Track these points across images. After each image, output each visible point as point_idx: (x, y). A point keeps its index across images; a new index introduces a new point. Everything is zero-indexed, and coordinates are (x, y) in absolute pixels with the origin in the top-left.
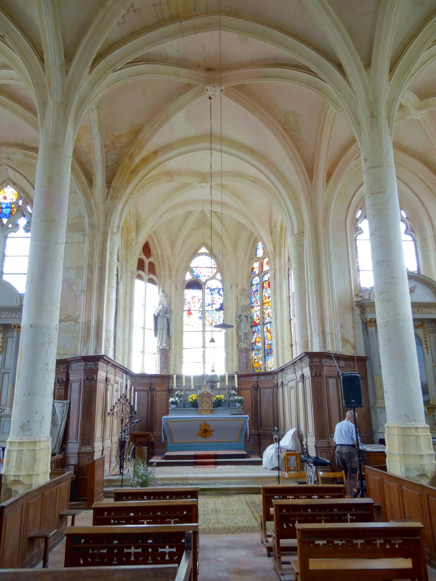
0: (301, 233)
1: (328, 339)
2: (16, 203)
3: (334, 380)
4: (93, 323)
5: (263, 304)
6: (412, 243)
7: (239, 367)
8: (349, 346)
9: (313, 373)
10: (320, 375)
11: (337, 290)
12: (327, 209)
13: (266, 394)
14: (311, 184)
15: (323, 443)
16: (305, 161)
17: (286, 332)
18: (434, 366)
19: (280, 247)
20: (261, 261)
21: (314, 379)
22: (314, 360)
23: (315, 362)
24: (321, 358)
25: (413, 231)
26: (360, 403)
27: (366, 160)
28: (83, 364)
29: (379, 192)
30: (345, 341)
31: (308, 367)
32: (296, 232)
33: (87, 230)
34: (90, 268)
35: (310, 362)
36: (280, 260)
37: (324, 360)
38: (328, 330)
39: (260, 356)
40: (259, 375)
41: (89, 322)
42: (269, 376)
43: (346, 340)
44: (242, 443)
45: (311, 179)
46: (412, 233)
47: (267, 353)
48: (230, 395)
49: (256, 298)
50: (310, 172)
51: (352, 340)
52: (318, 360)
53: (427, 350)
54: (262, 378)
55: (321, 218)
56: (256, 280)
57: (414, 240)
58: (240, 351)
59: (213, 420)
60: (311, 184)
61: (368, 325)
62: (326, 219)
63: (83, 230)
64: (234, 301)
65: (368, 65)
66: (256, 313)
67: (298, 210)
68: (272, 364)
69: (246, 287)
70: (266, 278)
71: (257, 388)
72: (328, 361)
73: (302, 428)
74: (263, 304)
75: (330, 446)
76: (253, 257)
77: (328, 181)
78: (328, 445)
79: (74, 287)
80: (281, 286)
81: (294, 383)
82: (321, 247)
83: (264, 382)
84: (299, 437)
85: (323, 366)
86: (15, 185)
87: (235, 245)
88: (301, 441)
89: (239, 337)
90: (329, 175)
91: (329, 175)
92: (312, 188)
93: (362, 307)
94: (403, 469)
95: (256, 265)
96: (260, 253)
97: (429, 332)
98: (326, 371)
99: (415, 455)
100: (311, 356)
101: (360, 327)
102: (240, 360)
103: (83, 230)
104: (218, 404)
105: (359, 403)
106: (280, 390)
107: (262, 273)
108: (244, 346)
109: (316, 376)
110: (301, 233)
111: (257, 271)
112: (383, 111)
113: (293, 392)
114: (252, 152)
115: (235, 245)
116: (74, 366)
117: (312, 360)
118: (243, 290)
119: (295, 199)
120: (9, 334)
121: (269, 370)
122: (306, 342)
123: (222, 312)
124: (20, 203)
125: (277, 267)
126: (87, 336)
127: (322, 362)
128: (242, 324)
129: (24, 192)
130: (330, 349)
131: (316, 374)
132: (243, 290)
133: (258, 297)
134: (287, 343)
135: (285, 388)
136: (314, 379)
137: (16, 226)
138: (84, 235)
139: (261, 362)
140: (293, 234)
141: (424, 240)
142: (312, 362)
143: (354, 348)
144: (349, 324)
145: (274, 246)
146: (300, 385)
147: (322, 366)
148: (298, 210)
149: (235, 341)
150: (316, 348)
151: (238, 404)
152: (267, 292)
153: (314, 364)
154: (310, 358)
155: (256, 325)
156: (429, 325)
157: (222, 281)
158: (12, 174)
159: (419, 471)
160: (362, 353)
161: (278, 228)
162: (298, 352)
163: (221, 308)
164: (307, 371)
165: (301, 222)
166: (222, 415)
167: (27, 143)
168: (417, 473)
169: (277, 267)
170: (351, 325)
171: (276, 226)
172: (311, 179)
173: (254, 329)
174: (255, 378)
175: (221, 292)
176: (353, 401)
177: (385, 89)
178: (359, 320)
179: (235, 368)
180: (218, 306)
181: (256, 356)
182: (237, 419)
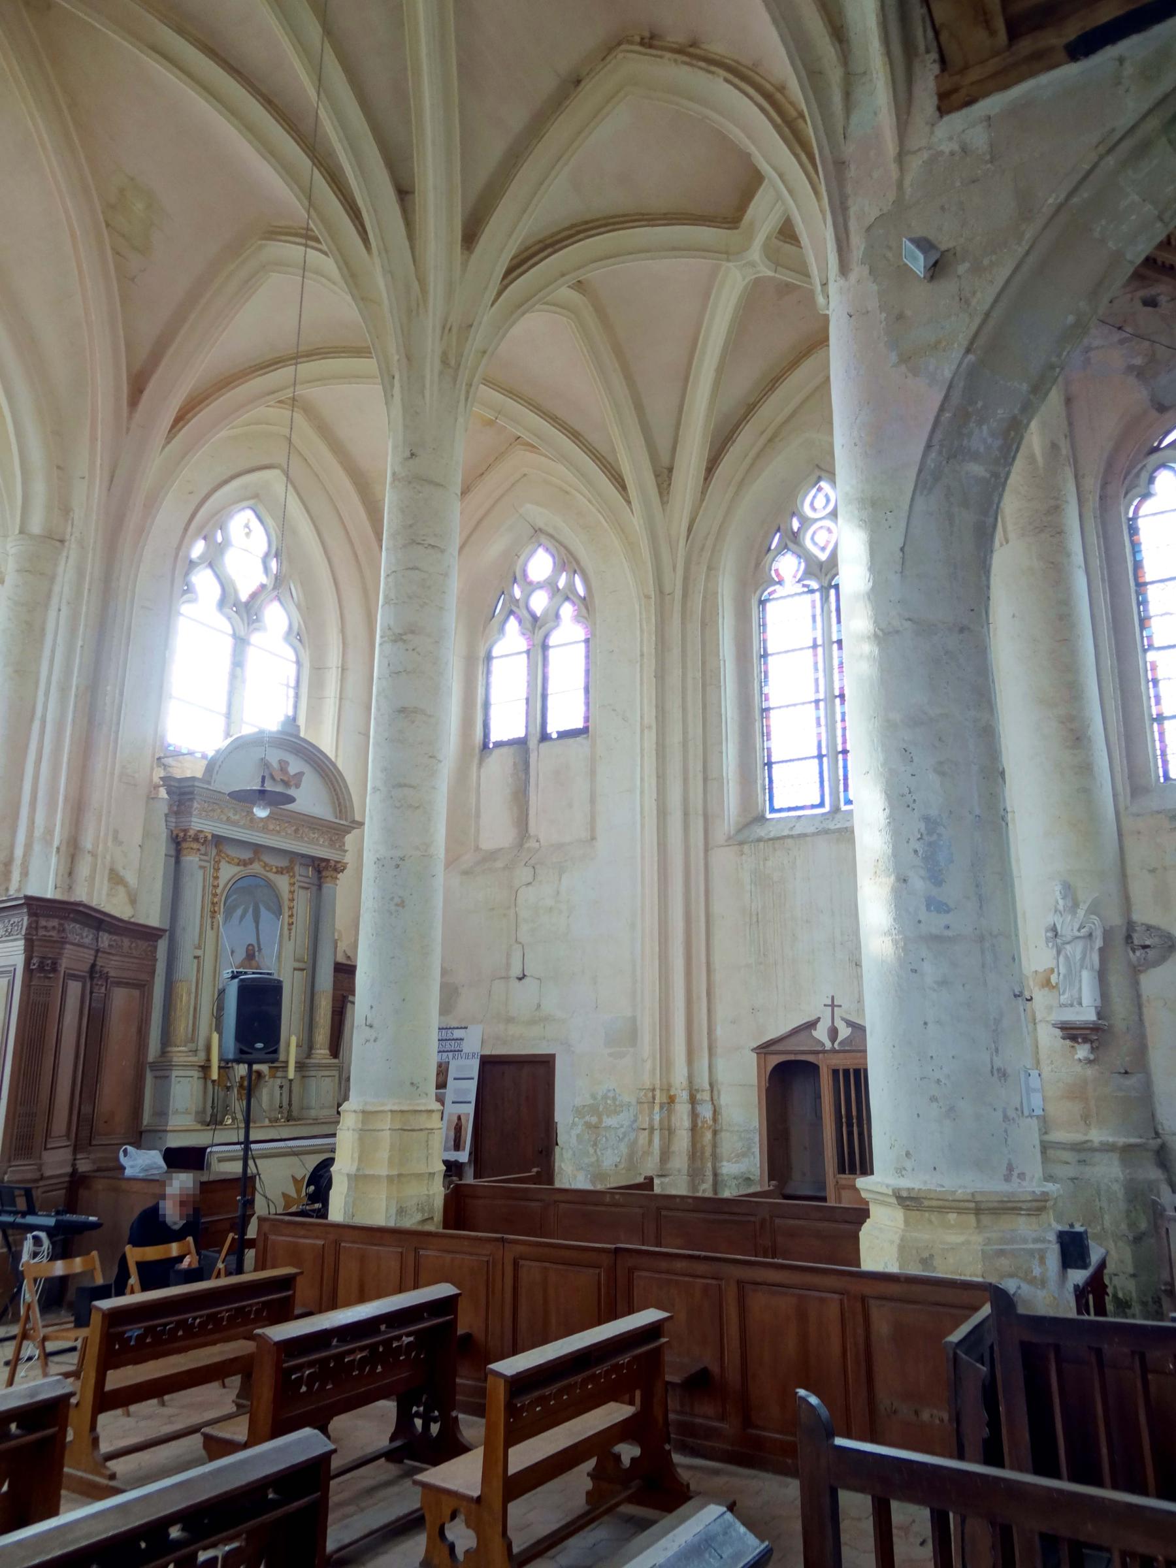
0: (54, 540)
1: (84, 869)
3: (79, 984)
6: (293, 668)
9: (35, 960)
10: (54, 969)
14: (130, 418)
18: (295, 969)
21: (31, 980)
22: (43, 922)
23: (45, 928)
24: (65, 918)
25: (300, 640)
26: (276, 1051)
27: (412, 455)
29: (433, 547)
31: (22, 942)
35: (29, 927)
37: (70, 926)
43: (117, 875)
45: (134, 402)
46: (297, 643)
51: (131, 878)
52: (55, 923)
53: (290, 930)
57: (298, 663)
60: (130, 418)
67: (58, 467)
72: (79, 931)
75: (42, 1178)
78: (36, 1175)
85: (65, 943)
90: (181, 419)
91: (181, 419)
92: (128, 429)
94: (393, 1211)
97: (301, 887)
99: (419, 1176)
100: (36, 907)
101: (161, 847)
109: (41, 967)
117: (37, 922)
119: (59, 435)
127: (64, 930)
130: (81, 894)
131: (41, 968)
136: (31, 980)
140: (21, 532)
141: (318, 669)
142: (36, 929)
143: (133, 901)
147: (63, 942)
153: (42, 932)
154: (32, 914)
156: (303, 871)
159: (423, 1211)
168: (419, 1217)
170: (137, 837)
172: (134, 402)
176: (260, 1045)
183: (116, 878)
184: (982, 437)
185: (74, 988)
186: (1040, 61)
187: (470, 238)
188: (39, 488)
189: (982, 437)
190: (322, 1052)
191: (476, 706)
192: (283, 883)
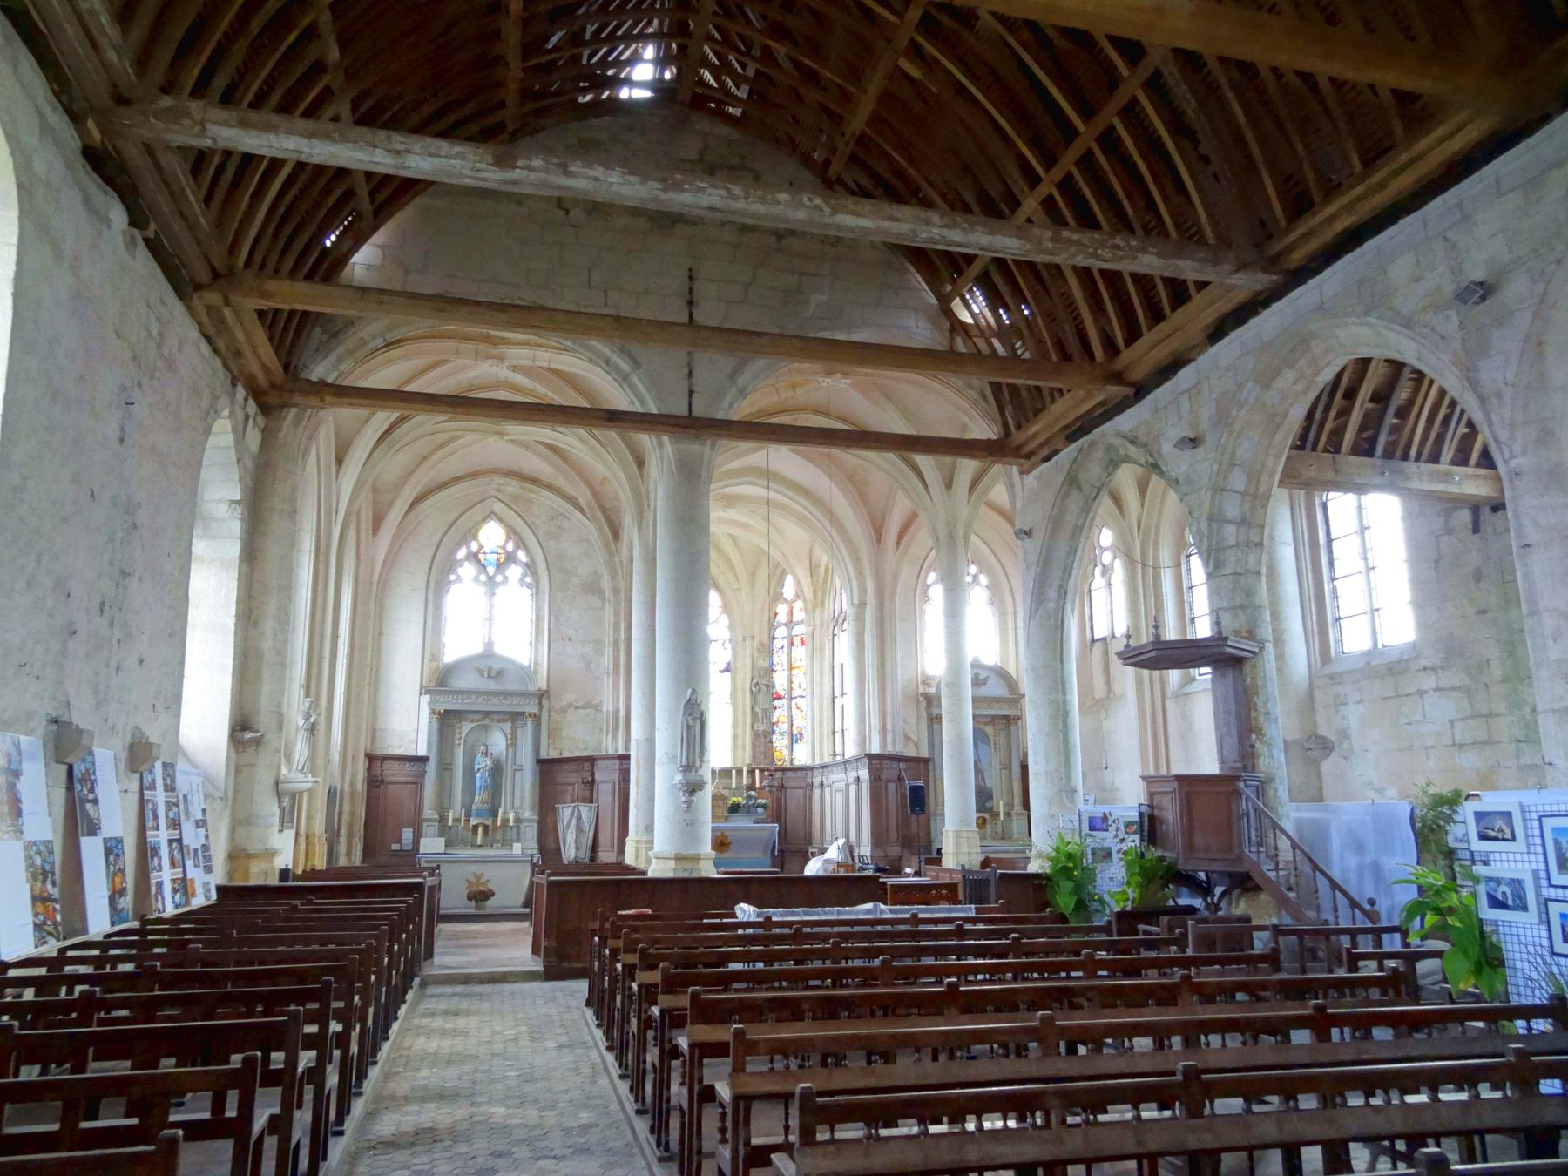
0: (863, 604)
2: (504, 547)
4: (622, 713)
5: (791, 669)
7: (754, 756)
8: (911, 746)
11: (902, 675)
12: (895, 577)
13: (794, 798)
15: (880, 853)
16: (873, 520)
17: (827, 714)
19: (824, 594)
20: (790, 603)
28: (617, 762)
30: (907, 739)
32: (856, 601)
33: (608, 594)
34: (616, 643)
36: (822, 612)
38: (889, 728)
39: (786, 741)
40: (784, 770)
41: (617, 712)
42: (799, 773)
44: (768, 860)
45: (879, 541)
47: (794, 739)
48: (750, 797)
49: (780, 658)
50: (878, 532)
51: (914, 738)
54: (790, 774)
55: (887, 591)
56: (781, 632)
58: (756, 735)
59: (728, 829)
61: (934, 720)
62: (894, 590)
63: (600, 593)
64: (748, 661)
65: (949, 485)
66: (780, 681)
68: (802, 756)
69: (766, 641)
70: (799, 630)
71: (782, 788)
73: (853, 837)
74: (791, 669)
76: (777, 597)
77: (898, 544)
79: (593, 666)
80: (822, 650)
81: (842, 785)
82: (884, 624)
83: (792, 780)
84: (849, 849)
86: (501, 520)
87: (753, 576)
88: (851, 852)
89: (754, 714)
91: (900, 537)
93: (929, 704)
95: (782, 609)
96: (789, 590)
98: (885, 775)
100: (871, 757)
101: (924, 723)
102: (754, 747)
103: (600, 593)
104: (735, 808)
105: (923, 810)
106: (817, 792)
107: (790, 624)
108: (762, 727)
109: (875, 778)
110: (863, 604)
111: (782, 617)
112: (961, 533)
113: (840, 796)
114: (806, 493)
115: (753, 576)
116: (600, 764)
118: (762, 644)
119: (857, 560)
120: (519, 723)
121: (797, 763)
122: (862, 740)
123: (728, 675)
124: (510, 547)
125: (818, 622)
126: (616, 728)
128: (761, 697)
129: (515, 533)
130: (890, 749)
132: (762, 644)
133: (784, 658)
134: (827, 729)
135: (827, 790)
137: (506, 578)
138: (603, 600)
139: (786, 752)
143: (917, 747)
144: (913, 720)
145: (815, 591)
146: (853, 788)
148: (860, 575)
149: (748, 720)
150: (875, 749)
151: (760, 810)
152: (799, 652)
155: (780, 698)
157: (731, 628)
158: (498, 507)
160: (925, 754)
161: (822, 569)
162: (851, 751)
163: (727, 670)
164: (864, 774)
165: (863, 590)
166: (741, 822)
167: (525, 472)
169: (818, 622)
171: (818, 566)
172: (879, 541)
173: (776, 703)
174: (778, 775)
175: (728, 645)
177: (964, 511)
178: (924, 714)
179: (746, 759)
180: (724, 666)
181: (780, 742)
182: (763, 829)
183: (907, 739)
184: (1052, 594)
185: (892, 786)
186: (1035, 466)
187: (949, 485)
188: (855, 583)
189: (1052, 594)
190: (1018, 807)
191: (1087, 622)
192: (989, 729)
